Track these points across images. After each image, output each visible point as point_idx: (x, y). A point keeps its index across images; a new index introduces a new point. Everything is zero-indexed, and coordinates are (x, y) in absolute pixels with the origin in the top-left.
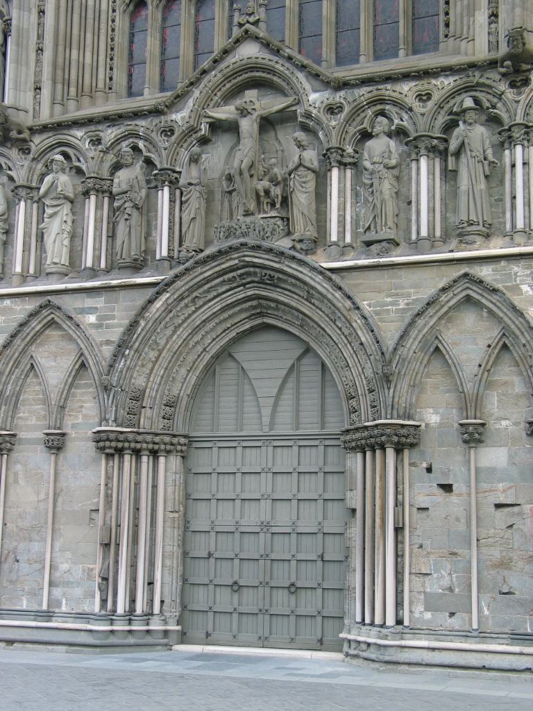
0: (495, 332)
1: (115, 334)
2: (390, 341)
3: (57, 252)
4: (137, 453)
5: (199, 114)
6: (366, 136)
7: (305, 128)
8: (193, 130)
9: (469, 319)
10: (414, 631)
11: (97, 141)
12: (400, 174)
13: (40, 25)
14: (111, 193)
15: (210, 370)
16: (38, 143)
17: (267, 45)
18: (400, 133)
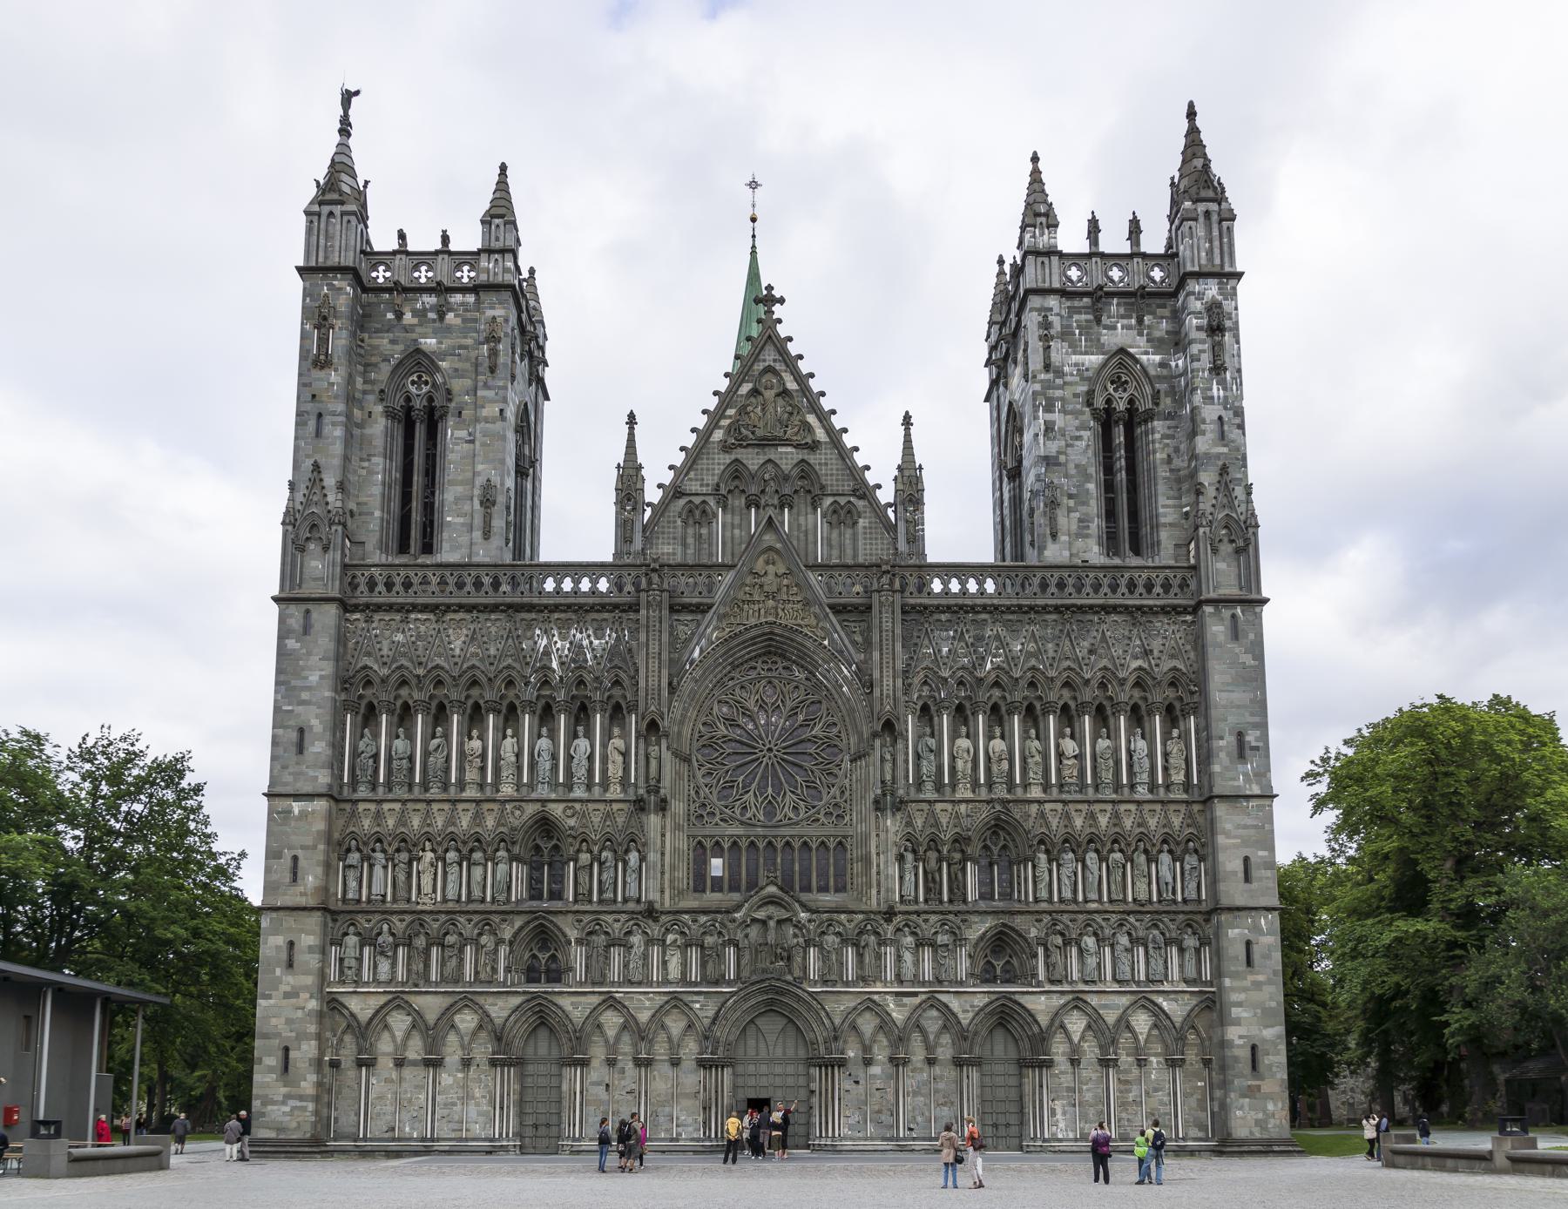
0: (878, 1021)
1: (711, 1013)
2: (837, 1021)
3: (674, 970)
4: (717, 1067)
5: (747, 915)
6: (823, 933)
7: (796, 926)
8: (745, 921)
9: (867, 1015)
10: (845, 1138)
11: (695, 921)
12: (839, 952)
13: (663, 860)
14: (702, 947)
15: (744, 1029)
16: (664, 918)
17: (781, 889)
18: (838, 934)
